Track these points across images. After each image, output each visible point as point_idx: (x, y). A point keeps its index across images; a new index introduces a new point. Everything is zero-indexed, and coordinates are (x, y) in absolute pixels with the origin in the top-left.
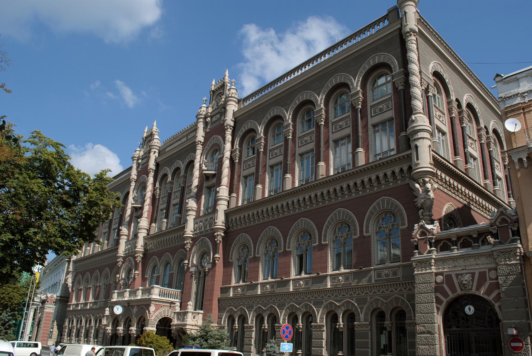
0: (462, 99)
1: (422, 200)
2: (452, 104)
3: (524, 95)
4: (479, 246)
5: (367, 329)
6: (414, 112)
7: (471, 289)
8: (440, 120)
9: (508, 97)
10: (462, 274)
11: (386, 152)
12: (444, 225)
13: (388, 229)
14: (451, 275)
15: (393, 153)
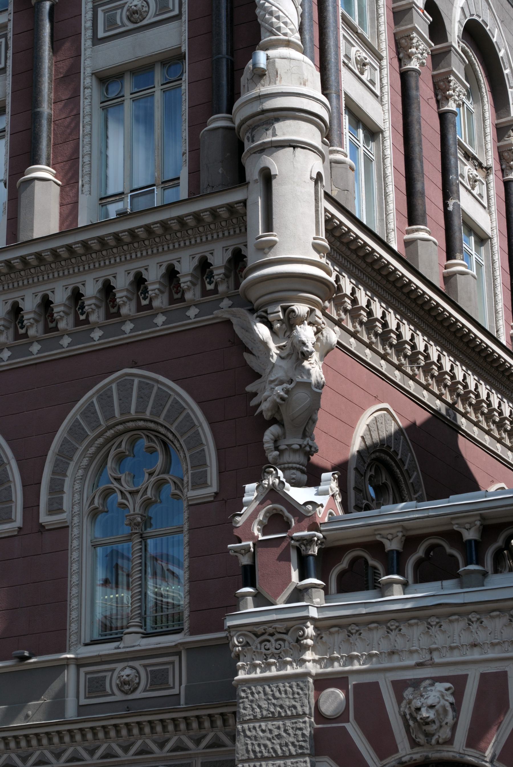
1: (279, 390)
2: (411, 21)
4: (485, 574)
6: (266, 38)
7: (450, 742)
10: (416, 683)
12: (355, 488)
13: (139, 499)
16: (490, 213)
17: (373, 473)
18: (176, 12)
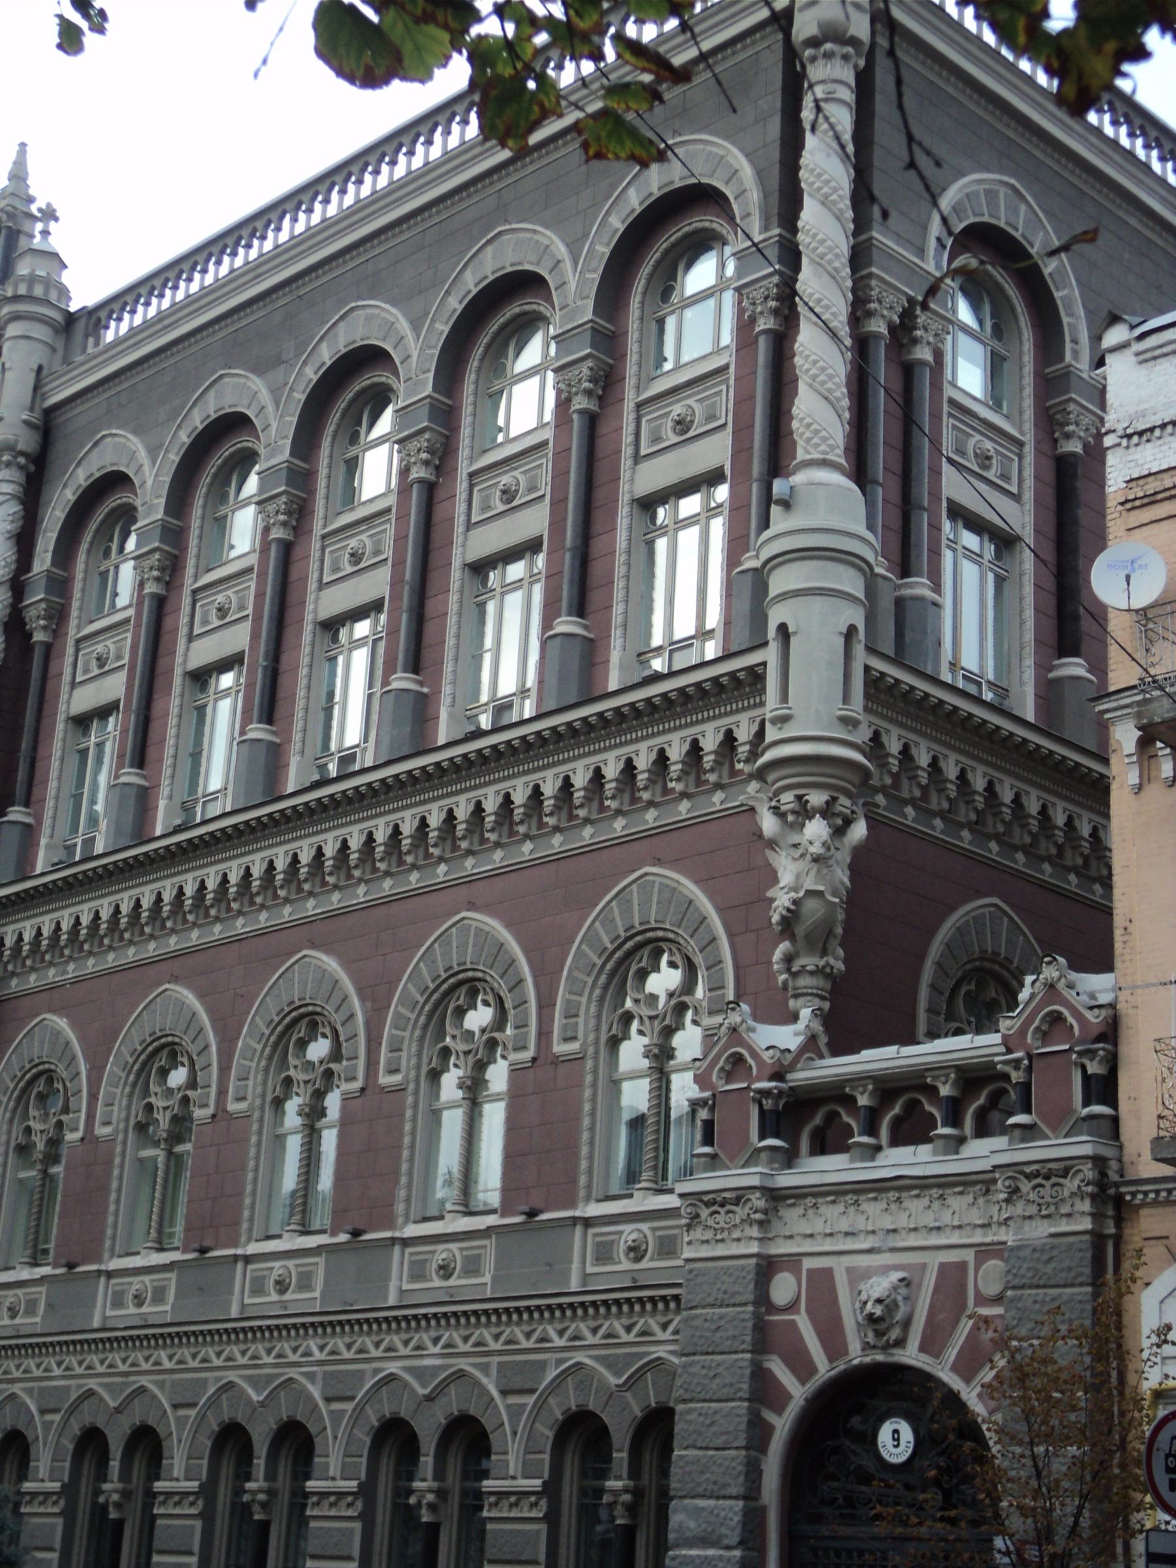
5: (533, 1514)
7: (900, 1343)
8: (990, 475)
9: (1141, 434)
11: (685, 644)
12: (929, 1010)
14: (828, 1273)
17: (972, 987)
18: (722, 421)
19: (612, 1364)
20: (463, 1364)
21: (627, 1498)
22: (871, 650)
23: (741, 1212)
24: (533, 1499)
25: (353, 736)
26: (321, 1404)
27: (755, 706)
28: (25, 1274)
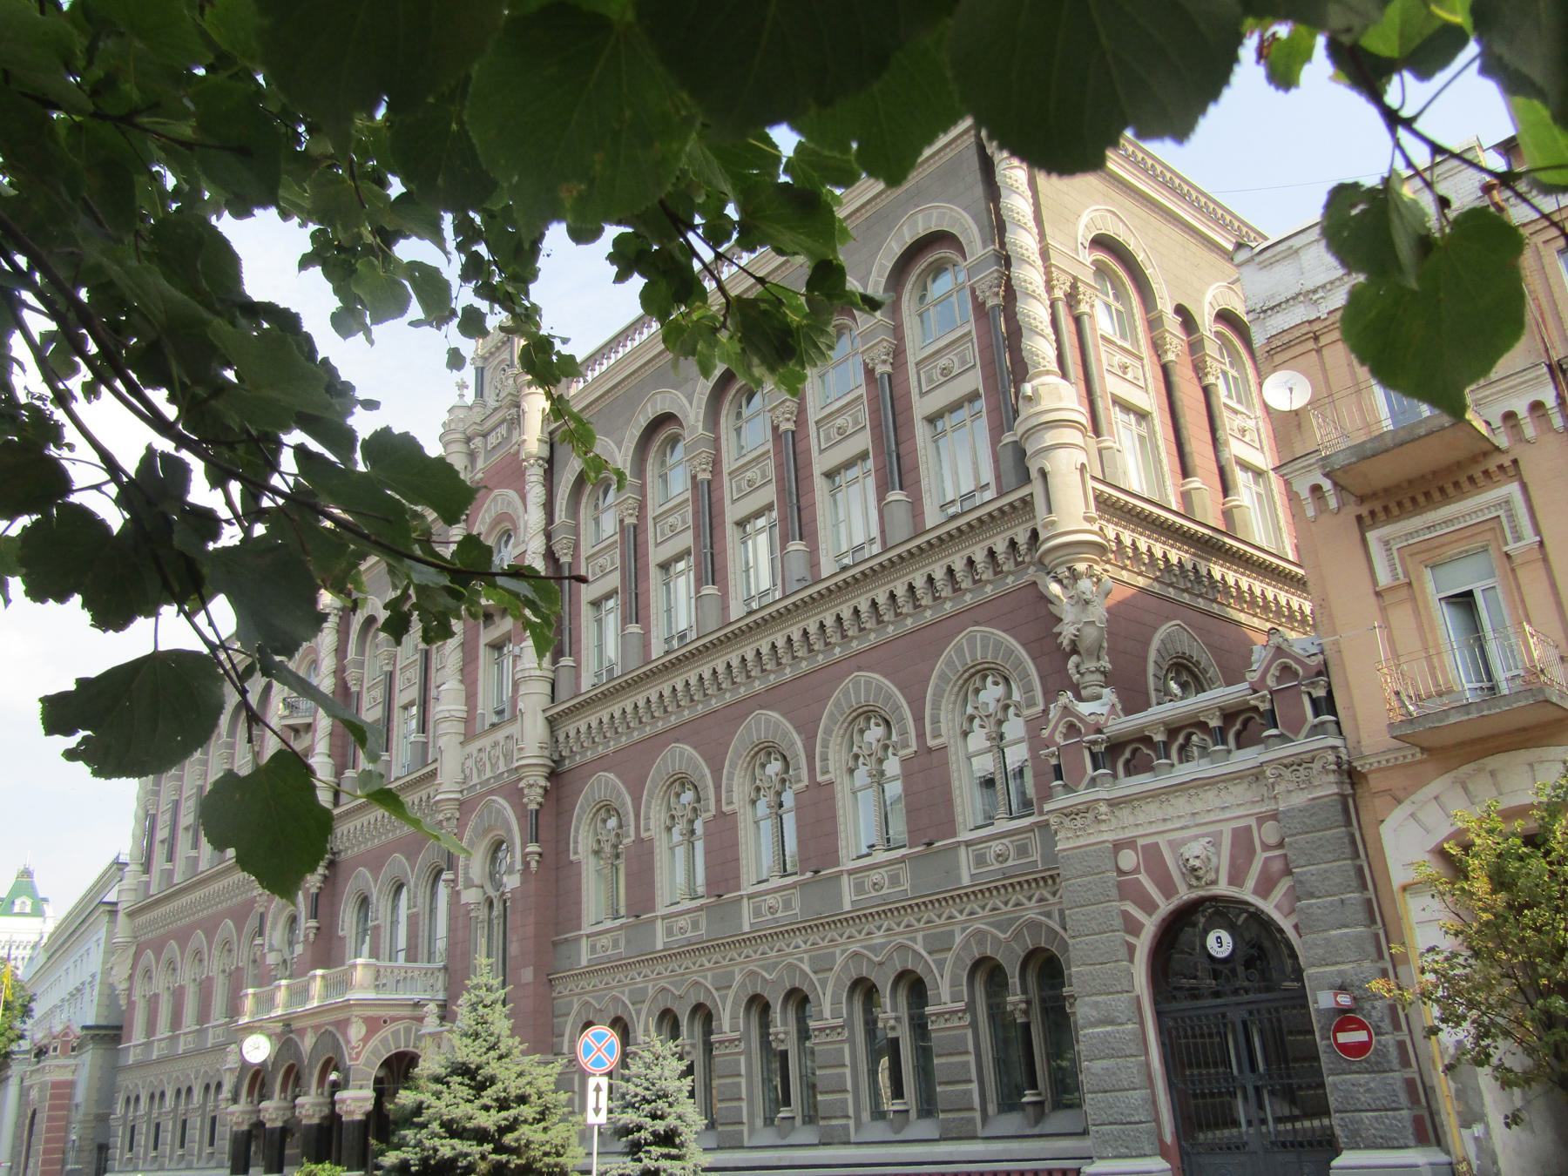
0: (1199, 302)
2: (1163, 325)
3: (1315, 298)
5: (962, 1023)
6: (1031, 371)
7: (1214, 882)
8: (1129, 377)
9: (1272, 309)
10: (1184, 842)
11: (970, 496)
14: (1157, 844)
15: (989, 495)
16: (1263, 452)
19: (999, 926)
20: (900, 939)
21: (1023, 1006)
22: (1093, 478)
23: (1090, 816)
24: (960, 1015)
25: (765, 583)
26: (812, 976)
27: (1030, 519)
28: (609, 924)
